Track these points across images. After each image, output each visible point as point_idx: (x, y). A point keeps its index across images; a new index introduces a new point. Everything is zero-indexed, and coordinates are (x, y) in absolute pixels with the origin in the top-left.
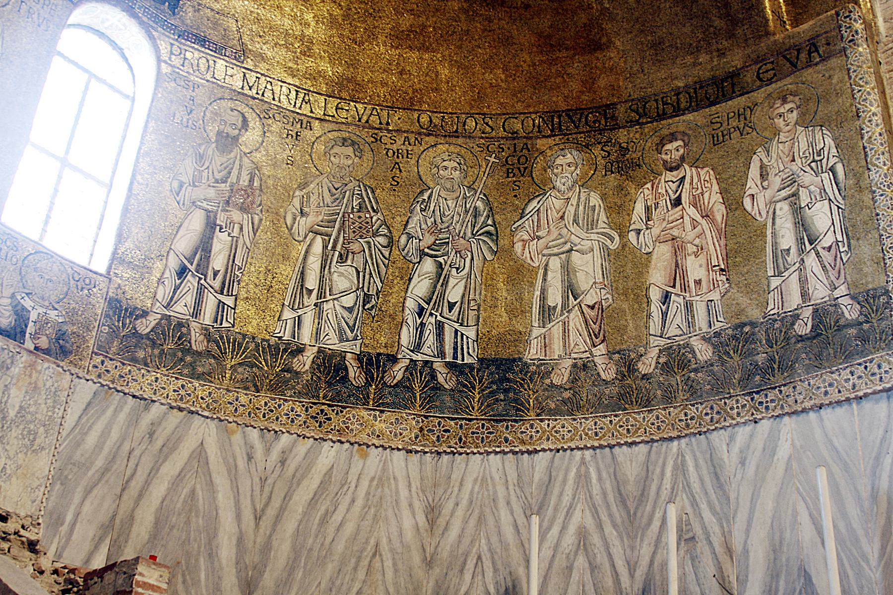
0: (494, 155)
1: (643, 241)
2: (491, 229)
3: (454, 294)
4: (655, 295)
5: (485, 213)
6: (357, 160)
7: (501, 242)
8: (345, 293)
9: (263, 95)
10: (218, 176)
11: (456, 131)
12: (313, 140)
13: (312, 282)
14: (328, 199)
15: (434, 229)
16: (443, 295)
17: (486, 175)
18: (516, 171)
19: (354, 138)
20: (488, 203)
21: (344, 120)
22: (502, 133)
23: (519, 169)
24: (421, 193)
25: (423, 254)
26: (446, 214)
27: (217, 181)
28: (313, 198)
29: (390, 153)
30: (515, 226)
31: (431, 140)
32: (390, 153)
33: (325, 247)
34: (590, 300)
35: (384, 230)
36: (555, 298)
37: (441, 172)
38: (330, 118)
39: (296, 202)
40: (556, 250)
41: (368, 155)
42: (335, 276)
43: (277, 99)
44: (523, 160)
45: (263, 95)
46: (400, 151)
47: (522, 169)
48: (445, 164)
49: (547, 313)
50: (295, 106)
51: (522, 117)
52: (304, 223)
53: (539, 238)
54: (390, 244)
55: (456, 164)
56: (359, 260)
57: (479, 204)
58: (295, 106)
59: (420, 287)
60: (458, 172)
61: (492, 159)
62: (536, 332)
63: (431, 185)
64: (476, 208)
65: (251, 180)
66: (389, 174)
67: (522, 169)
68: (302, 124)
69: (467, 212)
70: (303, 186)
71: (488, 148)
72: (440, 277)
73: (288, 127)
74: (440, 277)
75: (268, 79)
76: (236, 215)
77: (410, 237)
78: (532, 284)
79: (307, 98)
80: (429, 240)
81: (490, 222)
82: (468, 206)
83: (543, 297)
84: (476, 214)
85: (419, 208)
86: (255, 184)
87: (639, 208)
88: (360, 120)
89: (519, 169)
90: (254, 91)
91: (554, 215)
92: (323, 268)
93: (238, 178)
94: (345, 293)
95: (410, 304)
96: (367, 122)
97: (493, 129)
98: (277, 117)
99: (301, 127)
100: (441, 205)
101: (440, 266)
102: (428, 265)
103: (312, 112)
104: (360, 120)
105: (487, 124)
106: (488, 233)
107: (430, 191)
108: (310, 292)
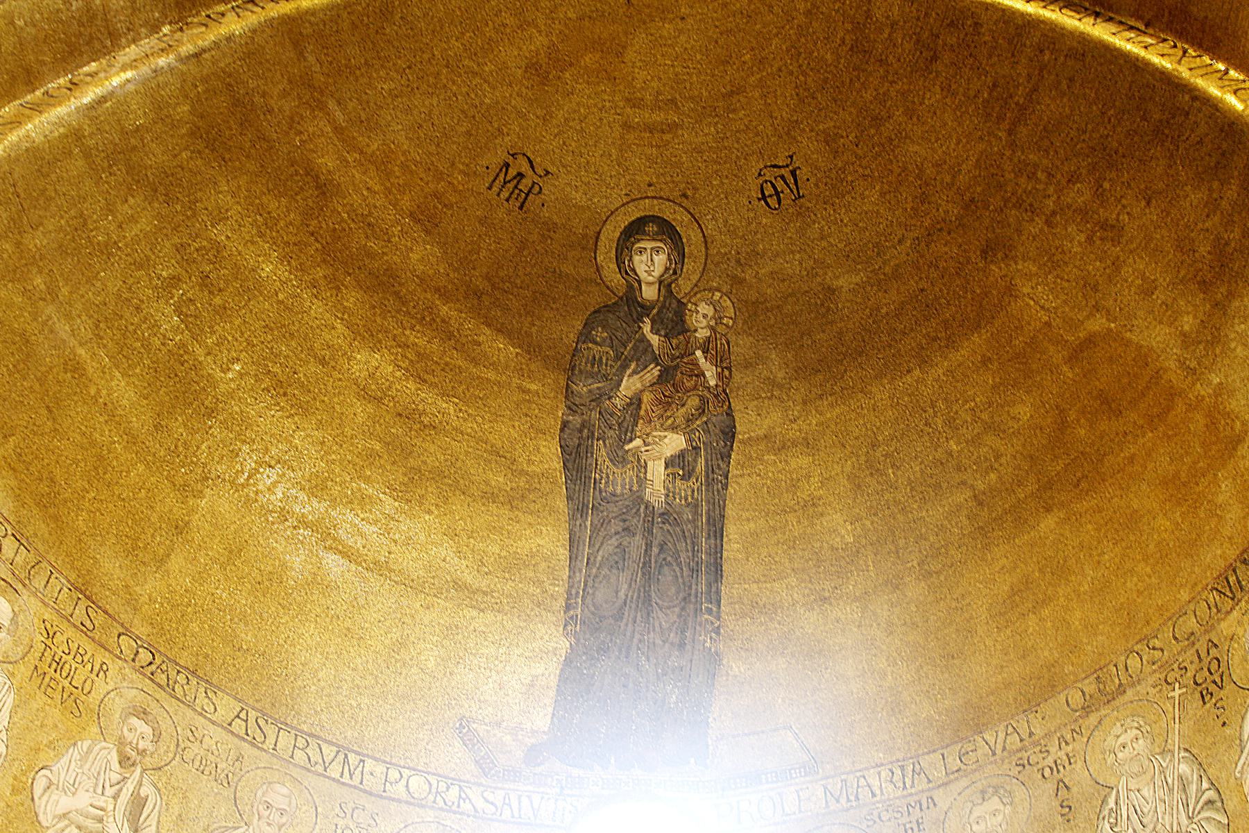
0: (1177, 685)
5: (1195, 777)
6: (1008, 809)
7: (1230, 806)
9: (857, 798)
11: (1121, 685)
12: (942, 818)
17: (1177, 720)
18: (1212, 688)
19: (995, 781)
21: (974, 766)
22: (1176, 647)
23: (1214, 682)
26: (1145, 810)
29: (1047, 772)
30: (1239, 768)
31: (1093, 719)
32: (1047, 772)
37: (1120, 755)
38: (956, 775)
41: (1020, 793)
43: (878, 792)
44: (1215, 664)
45: (857, 798)
46: (1059, 762)
47: (1218, 680)
48: (1121, 740)
50: (905, 787)
51: (1192, 606)
55: (1135, 732)
57: (1184, 768)
58: (905, 787)
60: (1141, 741)
61: (1177, 692)
63: (1112, 782)
64: (1180, 777)
66: (1056, 804)
67: (1218, 680)
68: (921, 805)
69: (1171, 790)
71: (1166, 681)
73: (904, 820)
75: (858, 774)
79: (917, 766)
81: (1205, 785)
82: (1170, 781)
85: (1107, 826)
88: (994, 754)
89: (1214, 682)
90: (843, 800)
96: (1004, 749)
97: (1162, 650)
98: (885, 816)
99: (921, 810)
100: (1136, 803)
103: (929, 781)
104: (994, 754)
105: (1154, 649)
106: (1210, 802)
107: (1114, 792)
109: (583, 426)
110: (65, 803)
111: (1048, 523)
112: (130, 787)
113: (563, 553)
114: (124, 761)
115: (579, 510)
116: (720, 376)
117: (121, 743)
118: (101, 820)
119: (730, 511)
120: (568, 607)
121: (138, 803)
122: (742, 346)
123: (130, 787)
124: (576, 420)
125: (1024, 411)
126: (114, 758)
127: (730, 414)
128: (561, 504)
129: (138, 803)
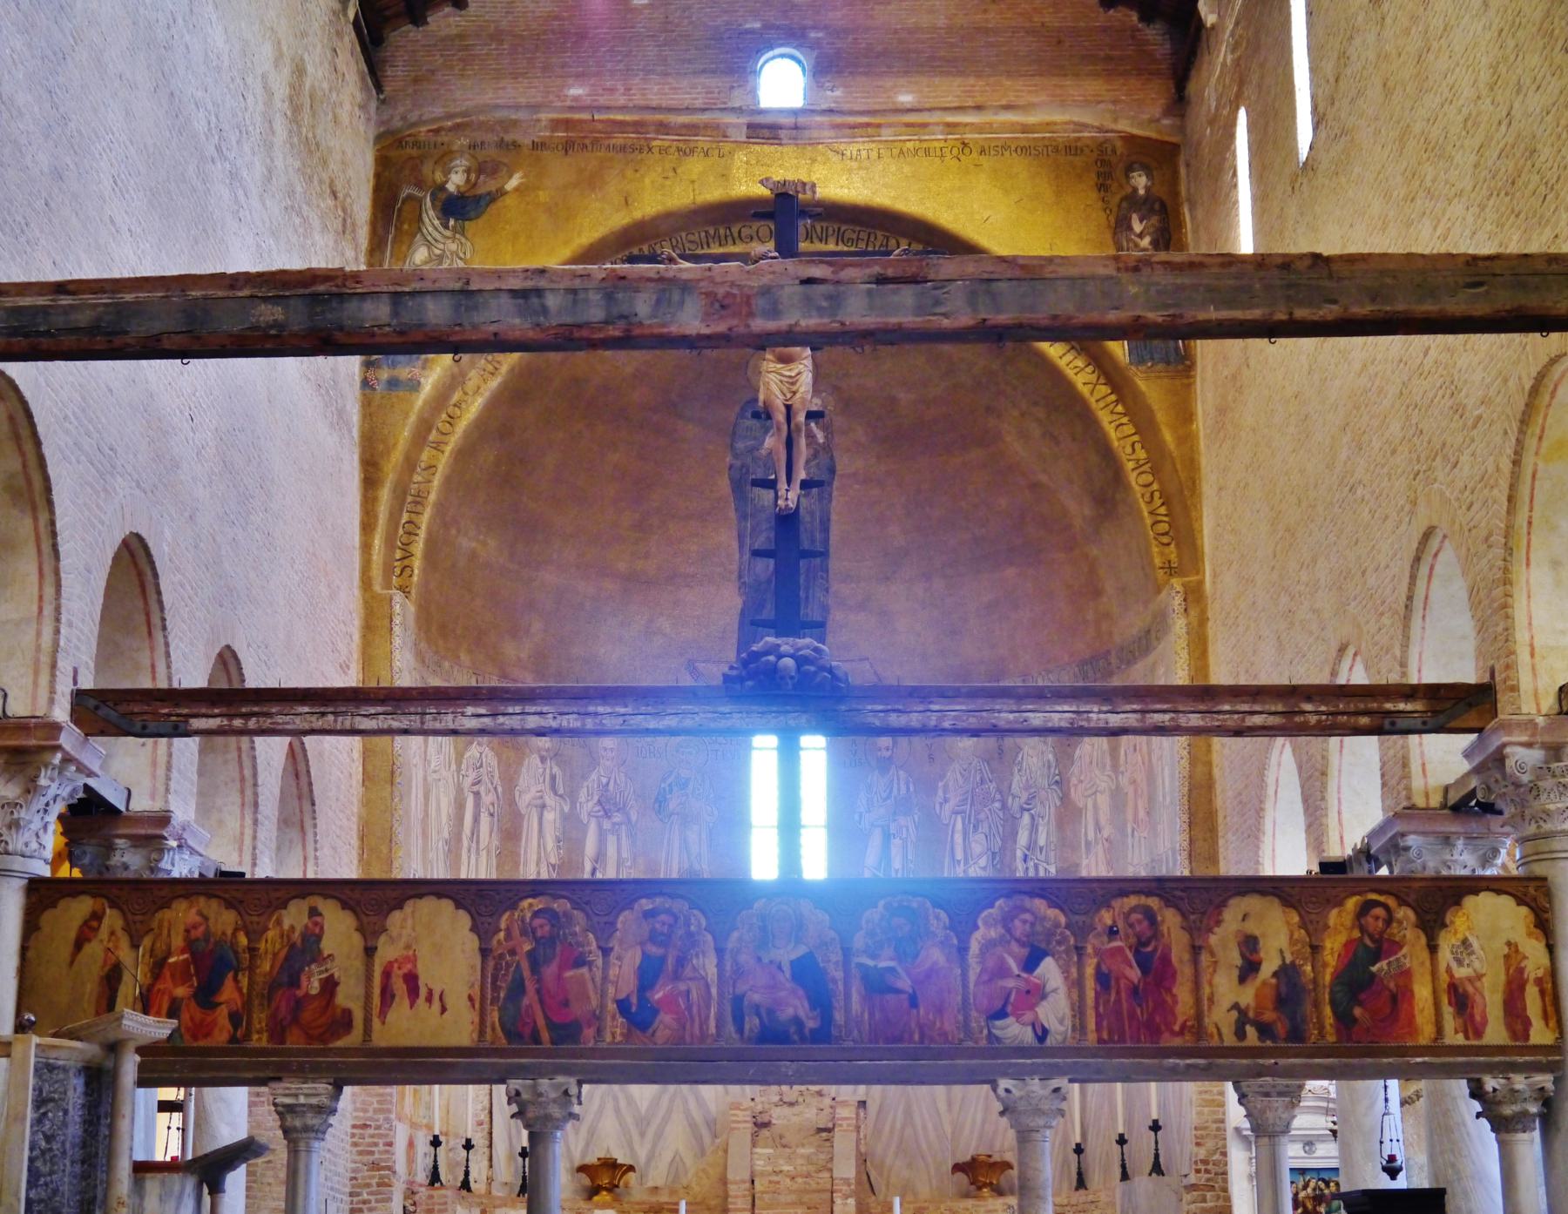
1: (1124, 781)
2: (1057, 778)
3: (1042, 841)
4: (1129, 831)
8: (980, 856)
10: (884, 795)
13: (959, 855)
14: (961, 781)
15: (1027, 787)
16: (1036, 842)
20: (1055, 755)
24: (1017, 756)
25: (1023, 810)
27: (885, 800)
28: (951, 784)
33: (963, 823)
34: (1106, 833)
35: (998, 797)
36: (1091, 835)
39: (940, 793)
40: (1090, 792)
42: (973, 845)
49: (1088, 844)
52: (948, 807)
53: (1081, 782)
54: (1004, 807)
56: (986, 825)
57: (1051, 757)
59: (1023, 838)
62: (1085, 862)
65: (908, 789)
70: (942, 777)
72: (1034, 828)
74: (1034, 828)
76: (902, 820)
77: (1014, 797)
78: (1080, 823)
80: (1025, 796)
83: (1086, 833)
84: (1049, 767)
86: (912, 789)
87: (1122, 753)
91: (1088, 760)
92: (964, 840)
93: (899, 790)
94: (980, 856)
95: (1019, 854)
101: (1033, 817)
102: (1026, 818)
108: (959, 862)
109: (743, 466)
110: (527, 798)
111: (1011, 572)
112: (548, 771)
113: (735, 544)
114: (543, 759)
115: (743, 517)
116: (826, 437)
117: (539, 751)
118: (541, 797)
119: (834, 517)
120: (740, 577)
121: (553, 778)
122: (839, 421)
123: (548, 771)
124: (738, 463)
125: (1003, 502)
126: (538, 761)
127: (832, 458)
128: (732, 515)
129: (553, 778)
